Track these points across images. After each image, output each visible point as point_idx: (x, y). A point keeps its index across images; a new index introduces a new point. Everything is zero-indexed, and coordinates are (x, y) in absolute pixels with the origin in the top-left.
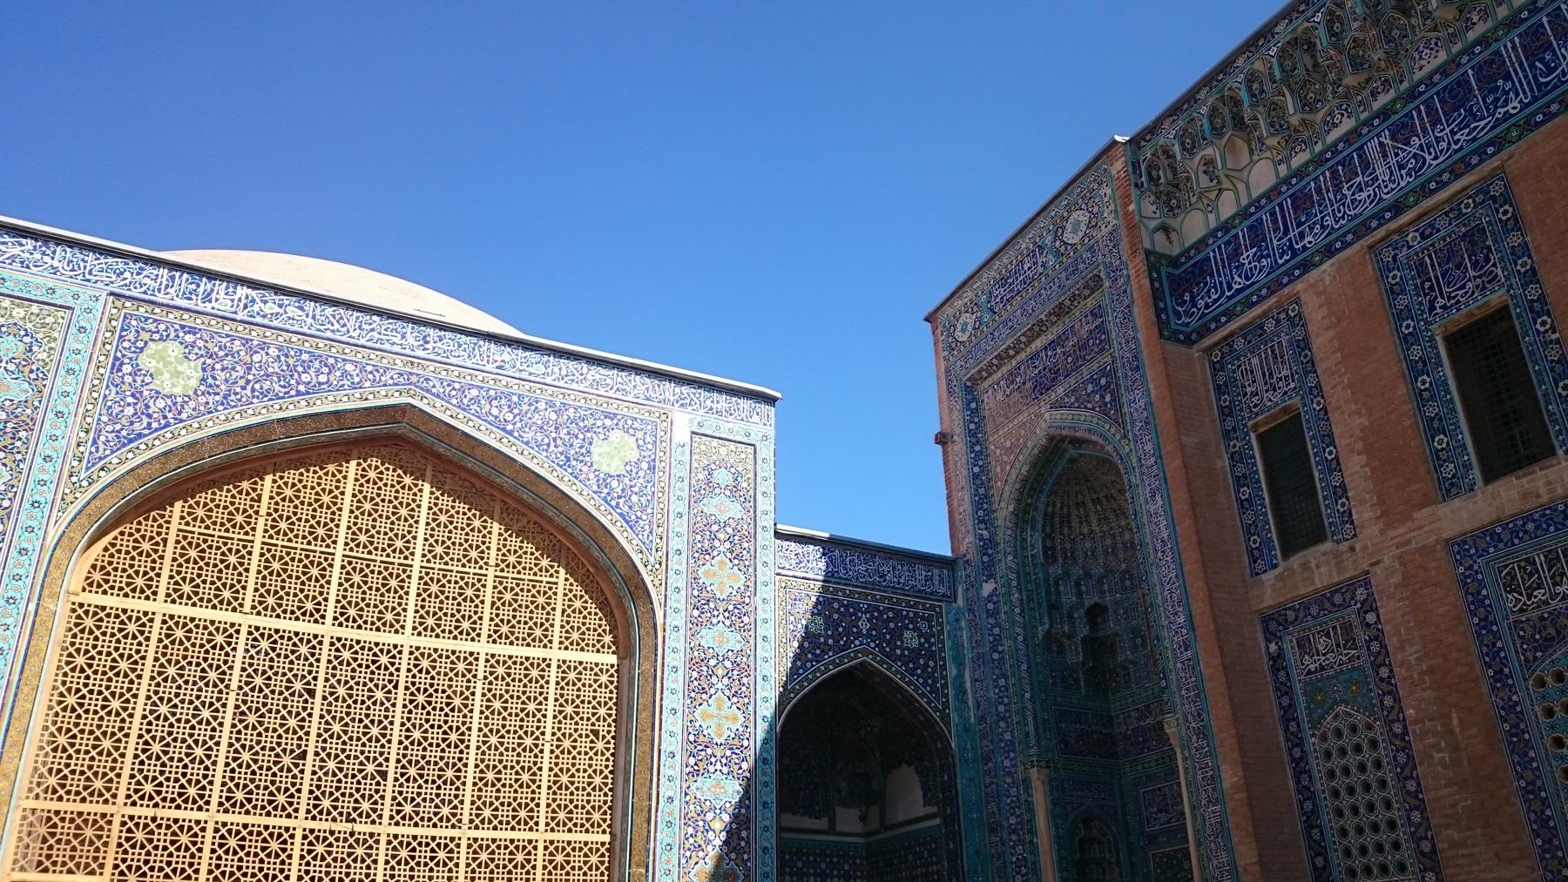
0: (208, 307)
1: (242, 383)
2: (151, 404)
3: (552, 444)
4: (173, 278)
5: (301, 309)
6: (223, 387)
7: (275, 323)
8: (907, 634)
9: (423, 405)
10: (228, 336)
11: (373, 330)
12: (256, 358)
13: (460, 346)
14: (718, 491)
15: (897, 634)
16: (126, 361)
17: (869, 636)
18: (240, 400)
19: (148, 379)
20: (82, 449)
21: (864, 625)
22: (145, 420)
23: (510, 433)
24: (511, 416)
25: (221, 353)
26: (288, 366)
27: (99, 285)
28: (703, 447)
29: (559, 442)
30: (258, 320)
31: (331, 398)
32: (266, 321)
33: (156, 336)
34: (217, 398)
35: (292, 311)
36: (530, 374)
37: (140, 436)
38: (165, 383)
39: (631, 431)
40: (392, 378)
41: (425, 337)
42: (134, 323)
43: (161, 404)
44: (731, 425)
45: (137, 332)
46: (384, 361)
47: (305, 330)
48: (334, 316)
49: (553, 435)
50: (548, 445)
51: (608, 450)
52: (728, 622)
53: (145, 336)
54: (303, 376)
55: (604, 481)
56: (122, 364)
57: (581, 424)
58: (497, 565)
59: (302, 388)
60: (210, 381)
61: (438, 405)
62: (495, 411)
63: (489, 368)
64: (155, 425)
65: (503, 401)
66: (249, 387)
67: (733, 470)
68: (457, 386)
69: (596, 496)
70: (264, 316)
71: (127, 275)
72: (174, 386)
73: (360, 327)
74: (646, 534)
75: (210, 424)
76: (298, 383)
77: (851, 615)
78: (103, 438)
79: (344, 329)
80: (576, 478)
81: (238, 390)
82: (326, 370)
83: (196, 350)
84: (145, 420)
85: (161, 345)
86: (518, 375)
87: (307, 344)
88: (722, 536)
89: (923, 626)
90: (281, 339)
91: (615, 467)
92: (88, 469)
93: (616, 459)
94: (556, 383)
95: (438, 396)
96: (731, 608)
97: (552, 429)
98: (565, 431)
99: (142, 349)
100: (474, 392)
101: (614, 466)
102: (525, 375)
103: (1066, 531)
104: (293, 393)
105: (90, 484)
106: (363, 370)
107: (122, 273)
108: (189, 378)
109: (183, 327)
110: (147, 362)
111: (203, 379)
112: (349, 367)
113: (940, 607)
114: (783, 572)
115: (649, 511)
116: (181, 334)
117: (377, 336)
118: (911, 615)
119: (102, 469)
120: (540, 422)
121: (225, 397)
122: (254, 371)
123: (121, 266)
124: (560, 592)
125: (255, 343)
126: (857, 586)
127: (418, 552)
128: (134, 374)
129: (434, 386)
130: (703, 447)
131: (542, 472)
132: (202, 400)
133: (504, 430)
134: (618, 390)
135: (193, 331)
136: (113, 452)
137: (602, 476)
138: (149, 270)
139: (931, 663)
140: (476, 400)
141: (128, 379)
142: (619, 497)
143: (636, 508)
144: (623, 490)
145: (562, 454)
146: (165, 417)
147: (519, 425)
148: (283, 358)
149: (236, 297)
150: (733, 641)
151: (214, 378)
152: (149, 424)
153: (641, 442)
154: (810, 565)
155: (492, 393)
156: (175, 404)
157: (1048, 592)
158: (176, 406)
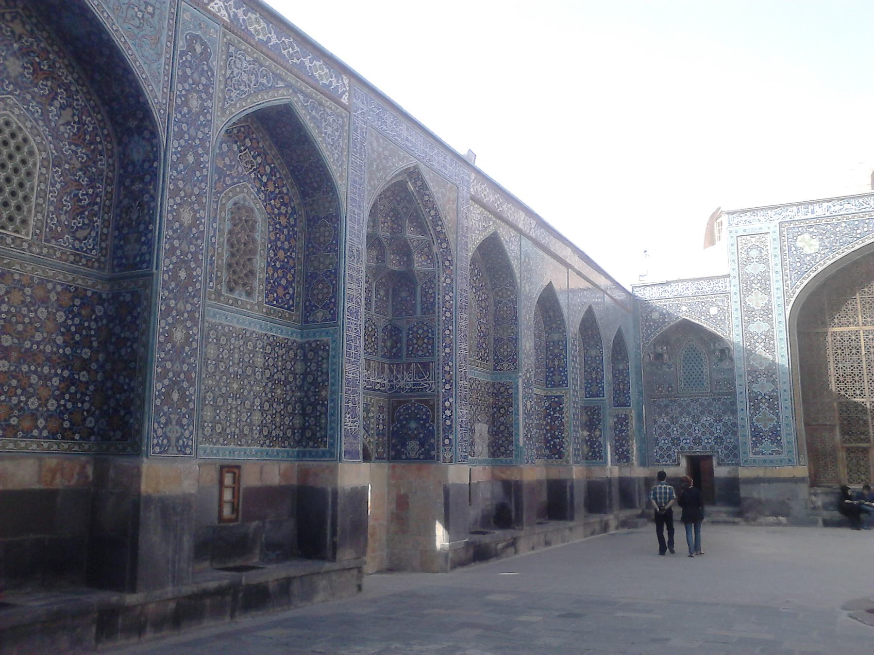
0: (814, 216)
1: (835, 241)
16: (792, 246)
22: (805, 266)
30: (834, 214)
34: (828, 250)
35: (847, 206)
38: (807, 250)
47: (854, 212)
59: (858, 236)
60: (823, 244)
70: (836, 212)
72: (811, 250)
78: (793, 277)
79: (869, 206)
81: (834, 244)
82: (866, 225)
85: (802, 236)
108: (815, 245)
132: (822, 252)
138: (790, 209)
141: (795, 253)
146: (811, 263)
148: (848, 226)
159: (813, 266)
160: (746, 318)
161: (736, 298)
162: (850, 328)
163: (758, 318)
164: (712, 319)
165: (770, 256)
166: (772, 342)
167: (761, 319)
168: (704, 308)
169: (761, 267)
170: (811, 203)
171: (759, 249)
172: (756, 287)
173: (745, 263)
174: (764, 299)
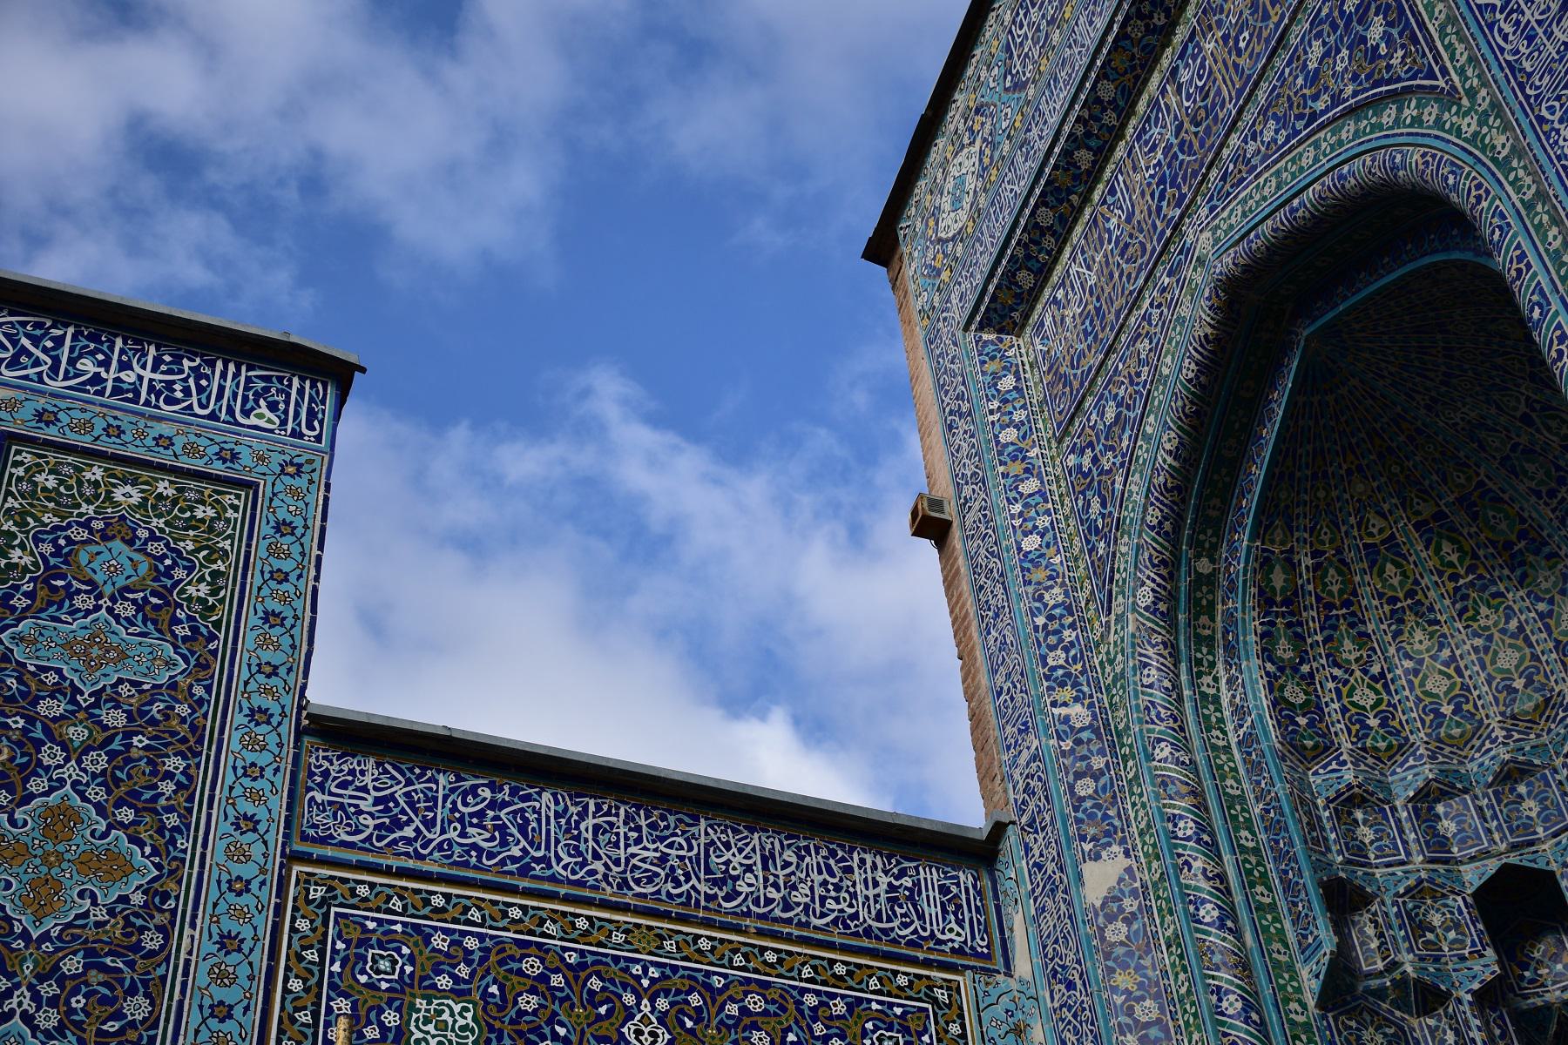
67: (156, 548)
77: (593, 999)
103: (1349, 652)
114: (317, 851)
118: (839, 1008)
126: (624, 908)
154: (435, 836)
157: (1316, 843)
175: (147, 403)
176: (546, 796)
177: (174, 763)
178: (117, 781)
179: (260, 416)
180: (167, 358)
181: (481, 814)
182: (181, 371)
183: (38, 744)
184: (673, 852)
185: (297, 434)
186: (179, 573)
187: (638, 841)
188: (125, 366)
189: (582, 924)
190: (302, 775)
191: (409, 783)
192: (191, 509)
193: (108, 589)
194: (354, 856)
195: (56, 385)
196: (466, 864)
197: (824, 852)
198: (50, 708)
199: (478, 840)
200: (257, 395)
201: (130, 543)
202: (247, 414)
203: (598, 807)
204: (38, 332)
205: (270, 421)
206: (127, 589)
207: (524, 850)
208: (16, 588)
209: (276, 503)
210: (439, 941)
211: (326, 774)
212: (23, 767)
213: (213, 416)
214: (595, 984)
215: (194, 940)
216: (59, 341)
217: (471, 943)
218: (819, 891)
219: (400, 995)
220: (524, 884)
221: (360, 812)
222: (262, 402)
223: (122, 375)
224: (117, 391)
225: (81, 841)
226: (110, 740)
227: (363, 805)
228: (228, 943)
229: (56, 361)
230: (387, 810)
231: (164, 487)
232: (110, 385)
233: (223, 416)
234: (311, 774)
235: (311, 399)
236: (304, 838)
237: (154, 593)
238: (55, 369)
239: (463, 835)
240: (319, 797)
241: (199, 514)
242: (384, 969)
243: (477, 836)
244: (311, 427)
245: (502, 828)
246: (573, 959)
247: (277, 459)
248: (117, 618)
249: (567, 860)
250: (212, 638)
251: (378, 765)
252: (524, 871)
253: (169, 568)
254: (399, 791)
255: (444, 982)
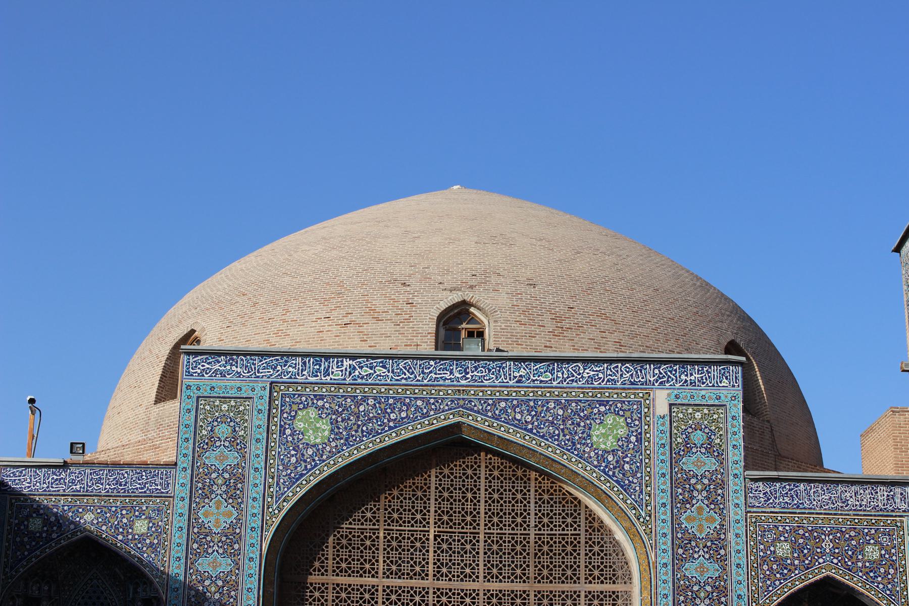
2: (305, 453)
3: (561, 434)
4: (305, 363)
5: (384, 367)
6: (344, 433)
7: (370, 381)
8: (869, 549)
9: (469, 421)
10: (342, 396)
11: (431, 372)
12: (362, 408)
13: (489, 371)
14: (694, 450)
15: (859, 549)
16: (287, 426)
17: (833, 554)
18: (355, 440)
19: (301, 437)
20: (272, 490)
21: (827, 545)
22: (303, 464)
23: (531, 431)
24: (530, 417)
25: (340, 410)
26: (381, 410)
27: (265, 379)
28: (681, 415)
29: (566, 432)
30: (359, 381)
31: (410, 428)
32: (364, 381)
33: (301, 406)
34: (342, 441)
35: (380, 370)
36: (541, 382)
37: (302, 475)
39: (621, 413)
40: (447, 405)
41: (465, 370)
42: (287, 400)
43: (310, 452)
44: (703, 393)
45: (290, 405)
46: (441, 393)
47: (389, 382)
48: (405, 368)
49: (562, 427)
50: (558, 435)
51: (603, 431)
52: (707, 556)
53: (295, 407)
54: (392, 415)
55: (602, 458)
56: (285, 429)
57: (582, 414)
58: (536, 526)
59: (391, 424)
60: (336, 430)
61: (479, 419)
62: (518, 416)
63: (511, 383)
64: (309, 467)
65: (523, 407)
66: (360, 430)
67: (707, 430)
68: (490, 402)
69: (596, 470)
70: (362, 378)
71: (279, 368)
72: (316, 438)
73: (423, 371)
74: (637, 494)
75: (340, 460)
76: (389, 421)
77: (815, 538)
78: (282, 481)
80: (581, 457)
81: (353, 433)
82: (405, 408)
83: (325, 411)
84: (303, 464)
86: (532, 384)
87: (391, 392)
88: (699, 487)
89: (885, 540)
90: (375, 391)
91: (610, 443)
92: (276, 502)
93: (610, 438)
94: (561, 385)
95: (478, 412)
96: (709, 544)
97: (560, 422)
98: (570, 422)
99: (294, 416)
100: (503, 404)
101: (609, 444)
102: (537, 383)
104: (387, 428)
105: (279, 511)
106: (428, 403)
107: (276, 367)
108: (324, 430)
109: (315, 396)
110: (300, 425)
111: (332, 430)
112: (419, 403)
113: (902, 522)
114: (752, 510)
115: (639, 475)
116: (315, 402)
117: (434, 376)
118: (873, 531)
119: (284, 501)
120: (551, 419)
121: (347, 440)
122: (361, 418)
123: (275, 362)
124: (583, 541)
125: (359, 398)
126: (821, 514)
127: (482, 523)
128: (292, 435)
129: (475, 406)
130: (681, 415)
131: (557, 458)
133: (525, 429)
134: (608, 381)
135: (321, 398)
136: (288, 489)
137: (600, 452)
139: (892, 571)
140: (504, 410)
142: (615, 468)
143: (629, 474)
144: (617, 462)
145: (568, 440)
146: (314, 460)
147: (536, 423)
149: (344, 368)
150: (713, 570)
151: (339, 428)
152: (306, 466)
153: (629, 421)
154: (777, 501)
155: (515, 402)
156: (318, 450)
158: (319, 452)
159: (316, 465)
160: (195, 546)
161: (182, 507)
162: (363, 579)
163: (216, 548)
164: (137, 542)
165: (248, 438)
166: (233, 593)
167: (221, 551)
168: (125, 520)
169: (232, 458)
170: (327, 357)
171: (232, 424)
172: (219, 492)
173: (205, 447)
174: (230, 514)
175: (698, 386)
176: (802, 485)
177: (720, 491)
178: (709, 498)
179: (724, 382)
180: (700, 369)
181: (787, 493)
182: (704, 372)
183: (692, 491)
184: (833, 496)
185: (733, 386)
186: (713, 437)
187: (824, 494)
188: (691, 375)
189: (812, 519)
190: (747, 490)
191: (770, 487)
192: (712, 416)
193: (699, 445)
194: (760, 510)
195: (677, 386)
196: (784, 508)
197: (871, 489)
198: (693, 481)
199: (787, 500)
200: (723, 375)
201: (701, 430)
202: (721, 382)
203: (814, 486)
204: (671, 369)
205: (727, 383)
206: (703, 444)
207: (798, 502)
208: (680, 449)
209: (731, 410)
210: (781, 529)
211: (752, 488)
212: (691, 497)
213: (713, 386)
214: (815, 534)
215: (731, 536)
216: (676, 370)
217: (787, 528)
218: (869, 500)
219: (773, 543)
220: (798, 511)
221: (760, 498)
222: (724, 377)
223: (691, 378)
224: (691, 383)
225: (705, 515)
226: (706, 487)
227: (761, 495)
228: (737, 535)
229: (676, 377)
230: (766, 496)
231: (706, 411)
232: (689, 382)
233: (716, 385)
234: (749, 489)
235: (736, 373)
236: (749, 506)
237: (709, 444)
238: (676, 380)
239: (783, 500)
240: (751, 495)
241: (714, 418)
242: (770, 537)
243: (787, 499)
244: (736, 383)
245: (792, 496)
246: (810, 528)
247: (730, 396)
248: (702, 453)
249: (807, 502)
250: (723, 454)
251: (763, 484)
252: (798, 507)
253: (710, 436)
254: (768, 490)
255: (782, 538)
